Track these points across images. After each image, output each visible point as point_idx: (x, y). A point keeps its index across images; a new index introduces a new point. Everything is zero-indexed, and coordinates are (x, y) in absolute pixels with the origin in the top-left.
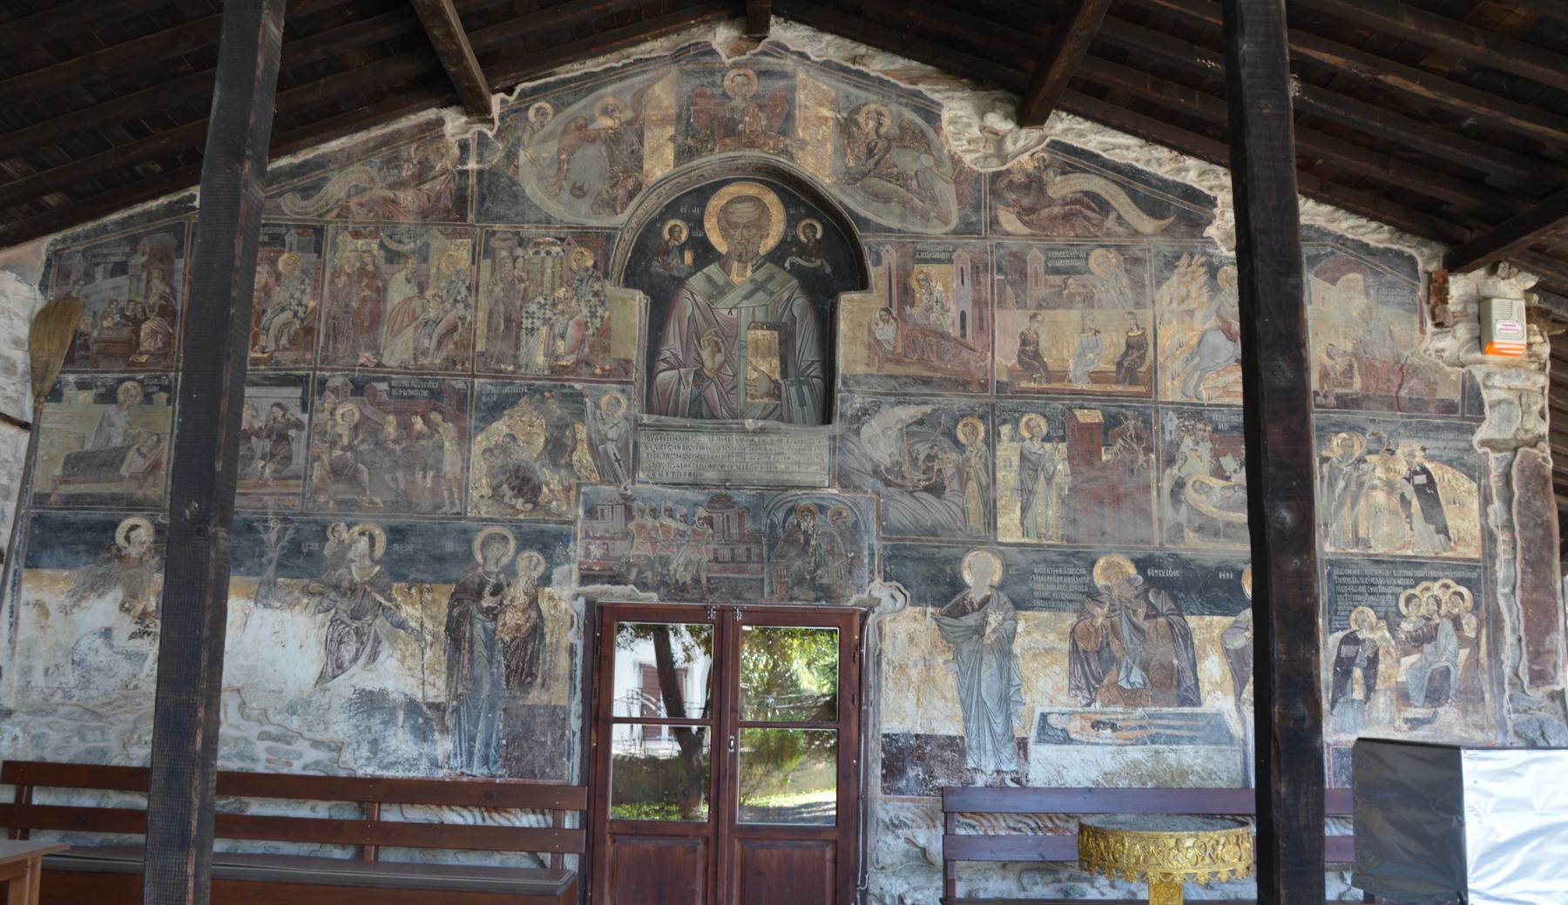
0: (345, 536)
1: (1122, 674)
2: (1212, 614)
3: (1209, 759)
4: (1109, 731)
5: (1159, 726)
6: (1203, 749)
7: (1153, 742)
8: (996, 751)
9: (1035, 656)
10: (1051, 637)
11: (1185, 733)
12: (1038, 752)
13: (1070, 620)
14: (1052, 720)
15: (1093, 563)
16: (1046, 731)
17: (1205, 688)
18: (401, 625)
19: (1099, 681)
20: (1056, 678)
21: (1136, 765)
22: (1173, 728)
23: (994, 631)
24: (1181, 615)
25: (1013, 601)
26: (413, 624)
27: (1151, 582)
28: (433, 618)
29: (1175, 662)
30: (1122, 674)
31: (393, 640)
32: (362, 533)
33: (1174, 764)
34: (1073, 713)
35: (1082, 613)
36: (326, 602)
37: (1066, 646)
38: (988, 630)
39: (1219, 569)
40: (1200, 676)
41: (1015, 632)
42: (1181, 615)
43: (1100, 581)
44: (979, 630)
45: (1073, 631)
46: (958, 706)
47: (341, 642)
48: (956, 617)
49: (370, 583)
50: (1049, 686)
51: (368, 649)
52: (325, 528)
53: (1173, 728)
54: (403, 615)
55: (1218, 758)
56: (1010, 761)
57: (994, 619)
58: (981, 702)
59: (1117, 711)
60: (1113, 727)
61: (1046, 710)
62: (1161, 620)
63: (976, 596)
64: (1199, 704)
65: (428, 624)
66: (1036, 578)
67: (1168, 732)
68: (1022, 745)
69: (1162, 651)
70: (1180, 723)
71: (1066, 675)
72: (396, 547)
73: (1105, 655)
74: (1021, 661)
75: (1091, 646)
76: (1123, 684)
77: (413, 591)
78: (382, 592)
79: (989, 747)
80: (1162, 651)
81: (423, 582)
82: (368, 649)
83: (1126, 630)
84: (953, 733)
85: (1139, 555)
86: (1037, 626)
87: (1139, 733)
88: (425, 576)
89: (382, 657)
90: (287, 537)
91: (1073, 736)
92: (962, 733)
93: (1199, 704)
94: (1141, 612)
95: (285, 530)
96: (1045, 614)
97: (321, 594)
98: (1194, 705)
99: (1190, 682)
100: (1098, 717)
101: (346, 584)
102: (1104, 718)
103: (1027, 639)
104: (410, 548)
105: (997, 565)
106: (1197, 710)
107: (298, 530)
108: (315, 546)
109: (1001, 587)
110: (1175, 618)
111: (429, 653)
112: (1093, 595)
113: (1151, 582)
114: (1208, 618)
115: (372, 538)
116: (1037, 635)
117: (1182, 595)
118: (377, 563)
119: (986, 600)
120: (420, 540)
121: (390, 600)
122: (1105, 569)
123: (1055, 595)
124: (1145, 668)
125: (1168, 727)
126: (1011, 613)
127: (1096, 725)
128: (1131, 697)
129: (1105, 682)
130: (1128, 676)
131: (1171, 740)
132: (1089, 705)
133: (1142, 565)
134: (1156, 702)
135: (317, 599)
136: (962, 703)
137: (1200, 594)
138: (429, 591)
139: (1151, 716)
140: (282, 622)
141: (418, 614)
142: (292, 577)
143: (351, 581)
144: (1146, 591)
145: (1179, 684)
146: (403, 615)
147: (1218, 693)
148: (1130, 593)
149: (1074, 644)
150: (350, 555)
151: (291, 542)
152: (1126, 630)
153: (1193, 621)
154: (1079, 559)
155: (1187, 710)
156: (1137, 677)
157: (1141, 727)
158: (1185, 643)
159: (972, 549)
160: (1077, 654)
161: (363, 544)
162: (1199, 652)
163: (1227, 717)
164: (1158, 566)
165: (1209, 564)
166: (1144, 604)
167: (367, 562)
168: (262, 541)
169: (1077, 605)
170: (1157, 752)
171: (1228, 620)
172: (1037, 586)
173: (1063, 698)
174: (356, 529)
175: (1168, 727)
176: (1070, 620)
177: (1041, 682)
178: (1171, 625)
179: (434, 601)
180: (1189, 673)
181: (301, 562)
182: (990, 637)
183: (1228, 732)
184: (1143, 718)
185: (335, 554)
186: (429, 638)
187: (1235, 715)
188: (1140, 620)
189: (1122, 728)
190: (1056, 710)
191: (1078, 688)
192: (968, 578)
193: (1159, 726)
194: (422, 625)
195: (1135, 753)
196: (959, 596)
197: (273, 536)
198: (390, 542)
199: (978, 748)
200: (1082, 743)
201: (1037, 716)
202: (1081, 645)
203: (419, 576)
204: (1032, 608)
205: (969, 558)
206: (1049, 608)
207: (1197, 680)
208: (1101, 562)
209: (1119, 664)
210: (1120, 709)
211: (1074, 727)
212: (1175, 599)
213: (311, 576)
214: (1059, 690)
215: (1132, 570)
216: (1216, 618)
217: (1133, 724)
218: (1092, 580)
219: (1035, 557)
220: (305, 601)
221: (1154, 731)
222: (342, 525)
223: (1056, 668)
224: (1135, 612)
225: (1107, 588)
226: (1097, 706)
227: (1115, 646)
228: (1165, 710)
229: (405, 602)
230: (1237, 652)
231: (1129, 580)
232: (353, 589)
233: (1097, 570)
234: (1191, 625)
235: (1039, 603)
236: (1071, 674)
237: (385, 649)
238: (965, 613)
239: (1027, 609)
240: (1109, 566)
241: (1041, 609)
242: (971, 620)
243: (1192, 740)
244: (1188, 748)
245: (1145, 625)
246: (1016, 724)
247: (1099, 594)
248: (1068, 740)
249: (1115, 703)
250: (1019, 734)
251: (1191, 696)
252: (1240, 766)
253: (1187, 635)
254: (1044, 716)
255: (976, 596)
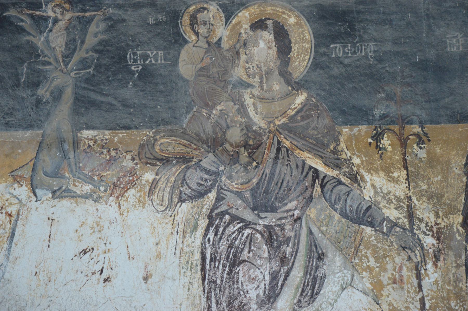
0: (222, 31)
18: (365, 216)
26: (392, 213)
28: (434, 197)
31: (352, 251)
32: (259, 25)
36: (195, 178)
47: (235, 262)
49: (288, 129)
51: (297, 274)
52: (175, 17)
54: (368, 194)
65: (425, 212)
72: (337, 50)
77: (385, 142)
78: (317, 148)
81: (406, 121)
82: (297, 274)
88: (407, 110)
89: (329, 289)
90: (91, 40)
95: (85, 23)
97: (184, 159)
101: (235, 135)
104: (369, 50)
107: (113, 24)
108: (157, 57)
111: (432, 275)
115: (281, 35)
118: (298, 86)
120: (388, 33)
121: (336, 164)
135: (174, 171)
138: (421, 140)
140: (98, 226)
141: (400, 190)
142: (115, 127)
143: (248, 127)
146: (368, 194)
150: (239, 72)
151: (102, 49)
161: (263, 47)
167: (277, 86)
168: (33, 52)
174: (244, 16)
179: (432, 161)
181: (129, 93)
185: (203, 71)
186: (429, 241)
194: (411, 216)
197: (58, 39)
198: (322, 40)
203: (393, 109)
213: (156, 122)
220: (149, 176)
222: (213, 8)
229: (371, 169)
232: (252, 146)
237: (335, 269)
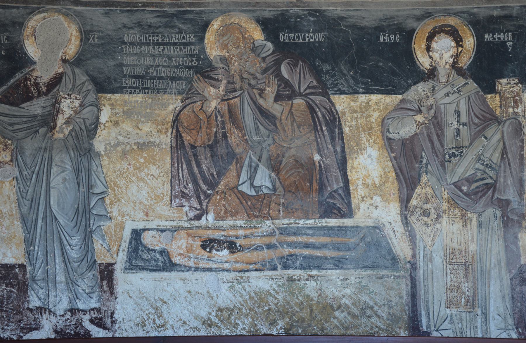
1: (244, 176)
2: (368, 91)
3: (362, 288)
4: (225, 252)
5: (290, 245)
6: (354, 275)
7: (286, 267)
8: (71, 283)
9: (124, 153)
10: (147, 128)
11: (329, 253)
12: (128, 282)
13: (172, 103)
14: (148, 239)
15: (206, 26)
16: (140, 255)
17: (358, 191)
19: (213, 185)
20: (154, 183)
21: (261, 297)
22: (314, 246)
23: (68, 122)
24: (326, 95)
25: (93, 80)
27: (284, 51)
29: (317, 158)
30: (244, 176)
33: (314, 295)
34: (176, 229)
35: (189, 95)
37: (166, 140)
38: (61, 120)
39: (380, 29)
40: (352, 176)
41: (96, 123)
42: (326, 95)
43: (213, 49)
44: (48, 121)
45: (176, 120)
46: (18, 224)
48: (16, 105)
50: (144, 193)
53: (314, 246)
55: (376, 287)
56: (89, 295)
57: (68, 106)
58: (50, 217)
59: (237, 226)
60: (232, 247)
61: (140, 226)
62: (298, 101)
63: (43, 74)
64: (349, 214)
66: (127, 49)
67: (306, 252)
68: (107, 274)
69: (302, 145)
70: (323, 240)
71: (167, 179)
73: (221, 150)
74: (105, 161)
75: (202, 138)
76: (245, 188)
79: (61, 277)
80: (302, 145)
83: (248, 116)
84: (10, 260)
85: (267, 14)
86: (127, 114)
87: (266, 254)
91: (177, 260)
92: (22, 260)
93: (349, 214)
94: (271, 91)
96: (139, 98)
98: (343, 216)
99: (336, 185)
100: (210, 234)
102: (218, 235)
103: (114, 132)
105: (72, 32)
106: (348, 222)
109: (78, 61)
110: (318, 99)
112: (204, 70)
113: (284, 51)
114: (363, 98)
116: (127, 126)
117: (326, 67)
119: (57, 80)
122: (221, 34)
123: (152, 72)
124: (275, 167)
125: (307, 246)
126: (91, 97)
127: (208, 244)
128: (256, 206)
129: (221, 186)
130: (252, 178)
131: (311, 263)
132: (198, 218)
133: (271, 27)
134: (289, 211)
136: (24, 219)
137: (352, 64)
139: (283, 231)
144: (278, 63)
145: (322, 188)
147: (377, 199)
148: (255, 66)
149: (178, 136)
152: (248, 116)
153: (342, 103)
154: (186, 21)
155: (332, 222)
156: (264, 179)
157: (270, 246)
158: (331, 132)
159: (32, 12)
160: (181, 150)
162: (350, 144)
163: (388, 231)
164: (295, 28)
165: (365, 23)
166: (275, 82)
169: (182, 85)
170: (291, 279)
171: (391, 100)
172: (128, 60)
173: (163, 209)
175: (307, 246)
176: (172, 103)
177: (134, 189)
178: (311, 109)
180: (335, 172)
182: (62, 129)
183: (390, 251)
184: (272, 234)
187: (400, 228)
188: (268, 102)
189: (242, 248)
190: (153, 225)
191: (184, 195)
192: (31, 49)
193: (290, 245)
195: (261, 282)
196: (19, 76)
199: (46, 280)
200: (189, 269)
201: (127, 234)
202: (187, 138)
204: (120, 90)
205: (34, 22)
206: (144, 89)
207: (347, 182)
208: (216, 25)
209: (239, 161)
210: (240, 223)
211: (178, 247)
212: (317, 73)
214: (158, 198)
215: (257, 35)
216: (374, 97)
217: (258, 241)
218: (203, 50)
219: (126, 19)
221: (286, 251)
223: (153, 169)
224: (262, 92)
225: (223, 59)
226: (210, 218)
227: (234, 138)
228: (302, 222)
230: (404, 142)
231: (254, 49)
233: (210, 37)
234: (339, 108)
235: (129, 82)
236: (174, 177)
238: (29, 98)
239: (113, 91)
240: (226, 30)
241: (132, 90)
242: (37, 107)
243: (338, 263)
244: (334, 274)
245: (276, 109)
246: (98, 245)
247: (214, 69)
248: (169, 265)
249: (234, 214)
250: (103, 258)
251: (339, 204)
252: (406, 299)
253: (334, 121)
254: (137, 234)
255: (43, 74)
